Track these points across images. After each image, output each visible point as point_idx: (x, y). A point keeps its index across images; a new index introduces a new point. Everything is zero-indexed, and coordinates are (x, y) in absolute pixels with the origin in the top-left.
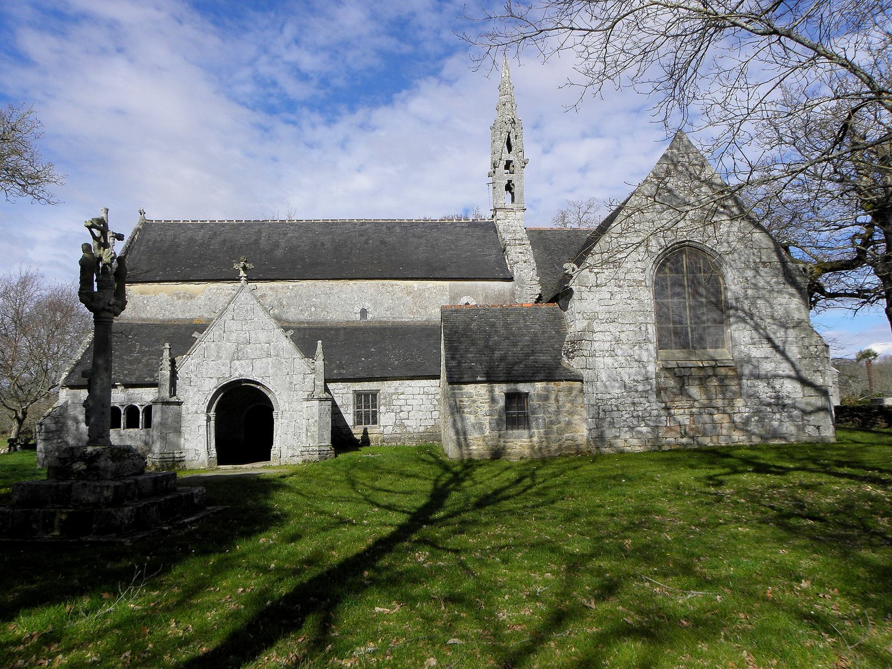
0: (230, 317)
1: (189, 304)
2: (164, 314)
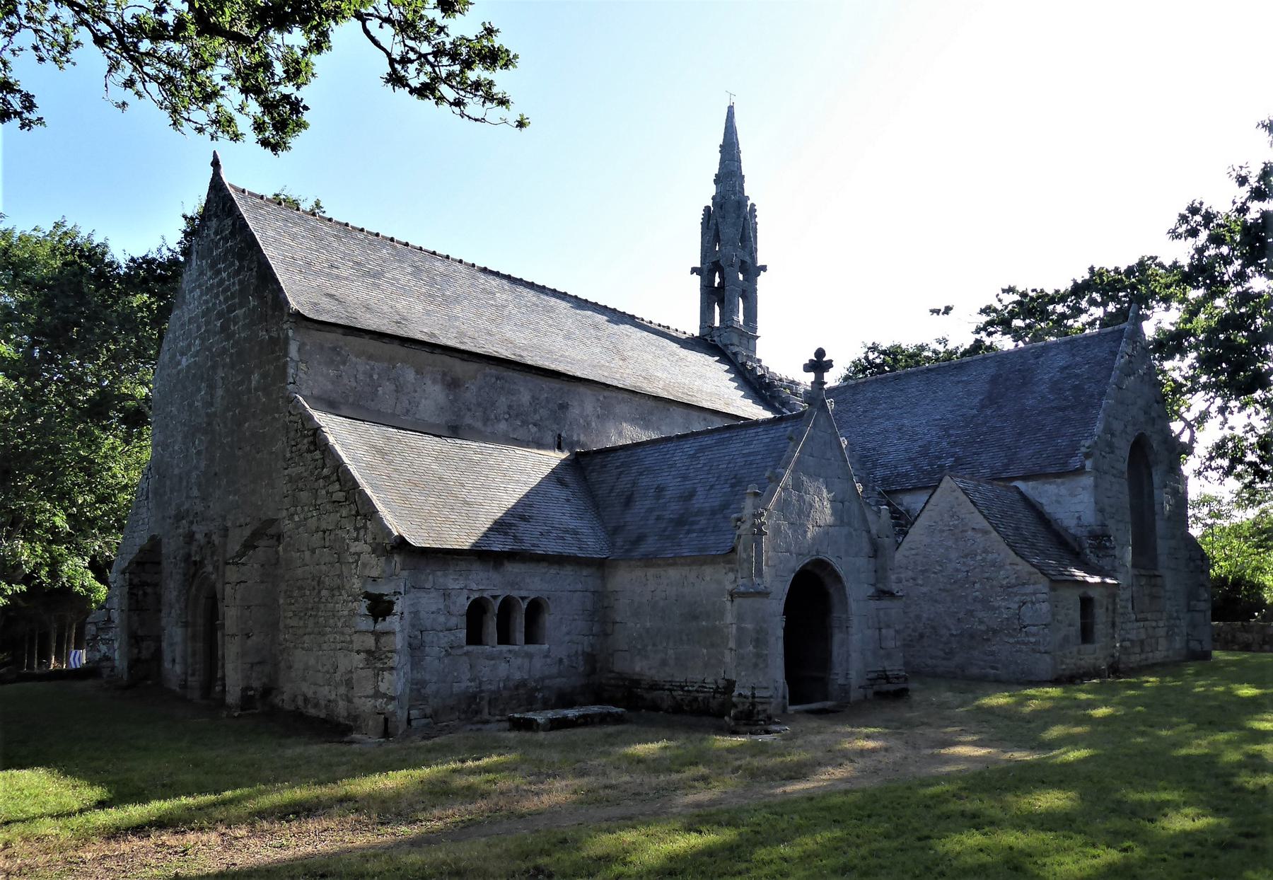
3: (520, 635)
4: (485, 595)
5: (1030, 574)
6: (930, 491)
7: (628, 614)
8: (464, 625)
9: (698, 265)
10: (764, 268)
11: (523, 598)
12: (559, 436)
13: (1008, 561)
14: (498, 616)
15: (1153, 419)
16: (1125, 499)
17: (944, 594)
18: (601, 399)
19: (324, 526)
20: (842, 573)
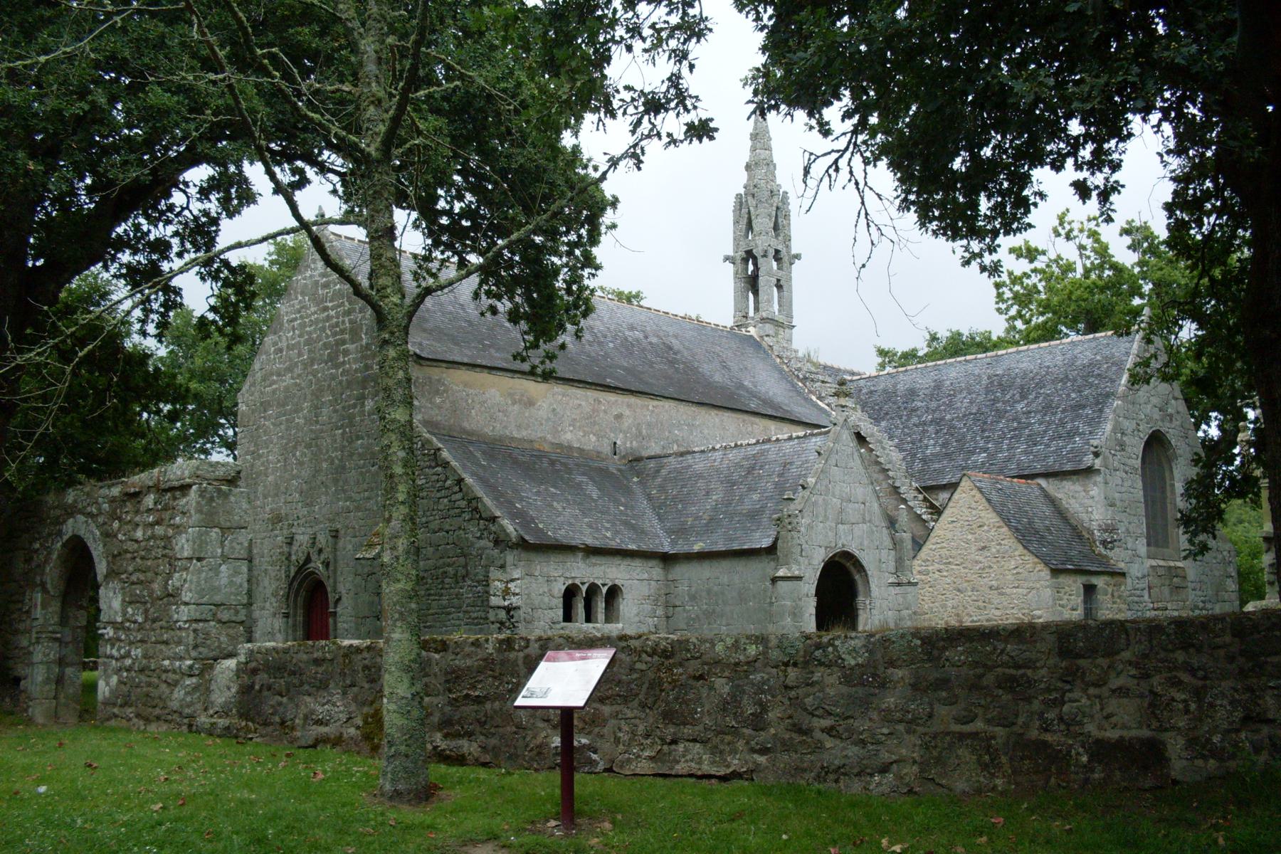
0: (834, 462)
1: (527, 414)
2: (494, 428)
3: (601, 615)
4: (577, 582)
5: (1036, 563)
6: (952, 490)
7: (687, 599)
8: (561, 605)
9: (731, 253)
10: (798, 257)
11: (604, 585)
12: (615, 443)
13: (1017, 553)
14: (585, 599)
15: (1171, 416)
16: (1139, 494)
17: (966, 584)
18: (651, 408)
19: (447, 527)
20: (864, 563)
